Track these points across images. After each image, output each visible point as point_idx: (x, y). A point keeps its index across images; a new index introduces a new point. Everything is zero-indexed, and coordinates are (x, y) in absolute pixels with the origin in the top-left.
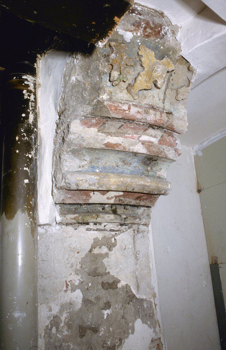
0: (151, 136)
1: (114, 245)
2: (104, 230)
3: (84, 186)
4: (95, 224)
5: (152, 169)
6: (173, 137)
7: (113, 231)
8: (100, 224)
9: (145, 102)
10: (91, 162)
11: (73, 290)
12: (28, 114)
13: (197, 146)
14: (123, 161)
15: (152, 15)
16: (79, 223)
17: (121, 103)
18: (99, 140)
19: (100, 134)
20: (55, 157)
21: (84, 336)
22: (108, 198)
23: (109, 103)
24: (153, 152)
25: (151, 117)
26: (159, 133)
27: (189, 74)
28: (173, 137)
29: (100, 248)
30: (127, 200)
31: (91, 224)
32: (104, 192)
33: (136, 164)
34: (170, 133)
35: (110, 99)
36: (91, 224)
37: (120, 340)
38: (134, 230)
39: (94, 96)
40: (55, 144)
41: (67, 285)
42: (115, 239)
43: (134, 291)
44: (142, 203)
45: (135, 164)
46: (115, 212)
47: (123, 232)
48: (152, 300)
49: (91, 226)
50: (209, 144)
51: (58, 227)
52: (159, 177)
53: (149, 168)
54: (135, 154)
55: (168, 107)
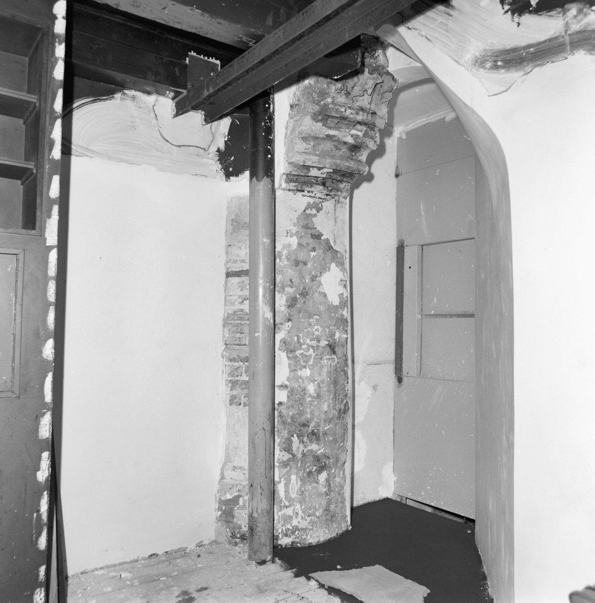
0: (358, 130)
1: (321, 209)
2: (314, 197)
3: (309, 163)
4: (309, 192)
5: (355, 154)
6: (374, 131)
7: (321, 198)
8: (312, 192)
9: (358, 104)
10: (314, 146)
11: (291, 236)
12: (269, 105)
13: (402, 127)
14: (336, 147)
15: (370, 42)
16: (297, 190)
17: (340, 106)
18: (323, 132)
19: (324, 127)
20: (286, 140)
21: (297, 266)
22: (322, 173)
23: (332, 106)
24: (358, 142)
25: (360, 118)
26: (364, 128)
27: (393, 83)
28: (374, 131)
29: (311, 210)
30: (335, 176)
31: (306, 192)
32: (320, 169)
33: (344, 149)
34: (373, 128)
35: (333, 103)
36: (306, 192)
37: (321, 273)
38: (336, 200)
39: (322, 98)
40: (286, 129)
41: (287, 233)
42: (322, 205)
43: (332, 244)
44: (345, 179)
45: (344, 150)
46: (324, 184)
47: (328, 200)
48: (344, 253)
49: (306, 193)
50: (414, 127)
51: (282, 192)
52: (360, 161)
53: (353, 154)
54: (345, 143)
55: (373, 107)
